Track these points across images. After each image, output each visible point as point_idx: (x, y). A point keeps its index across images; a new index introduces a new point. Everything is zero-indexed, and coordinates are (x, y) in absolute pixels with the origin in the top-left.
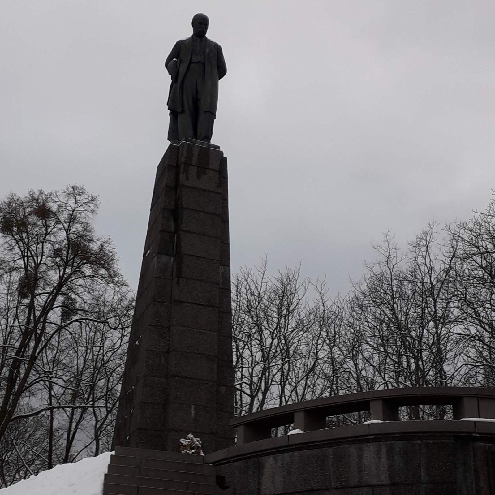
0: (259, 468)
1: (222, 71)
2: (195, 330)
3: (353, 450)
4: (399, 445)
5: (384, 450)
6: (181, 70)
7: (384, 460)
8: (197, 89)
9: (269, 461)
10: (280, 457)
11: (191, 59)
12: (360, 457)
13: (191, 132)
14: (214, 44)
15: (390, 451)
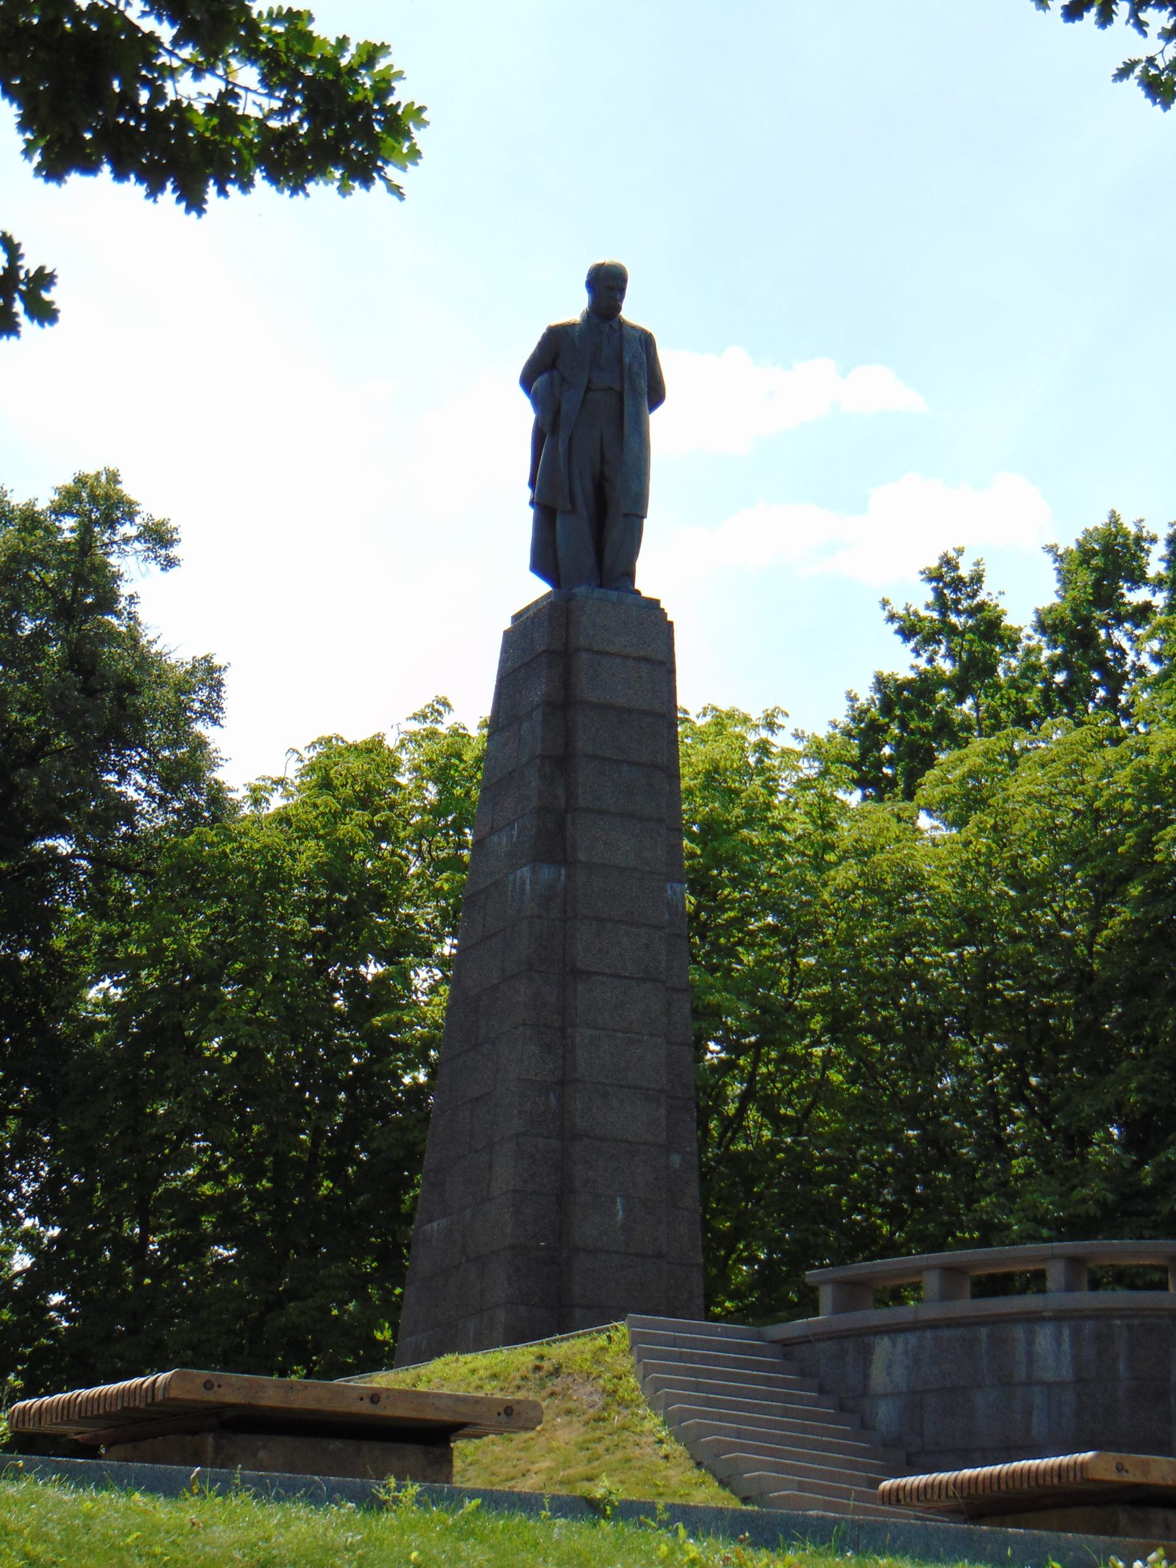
0: (866, 1354)
1: (656, 395)
2: (620, 1035)
3: (1019, 1332)
4: (1089, 1326)
5: (1066, 1332)
6: (565, 407)
7: (1066, 1346)
8: (602, 453)
9: (883, 1345)
10: (900, 1339)
11: (589, 381)
12: (1030, 1342)
13: (590, 560)
14: (637, 335)
15: (1076, 1334)
